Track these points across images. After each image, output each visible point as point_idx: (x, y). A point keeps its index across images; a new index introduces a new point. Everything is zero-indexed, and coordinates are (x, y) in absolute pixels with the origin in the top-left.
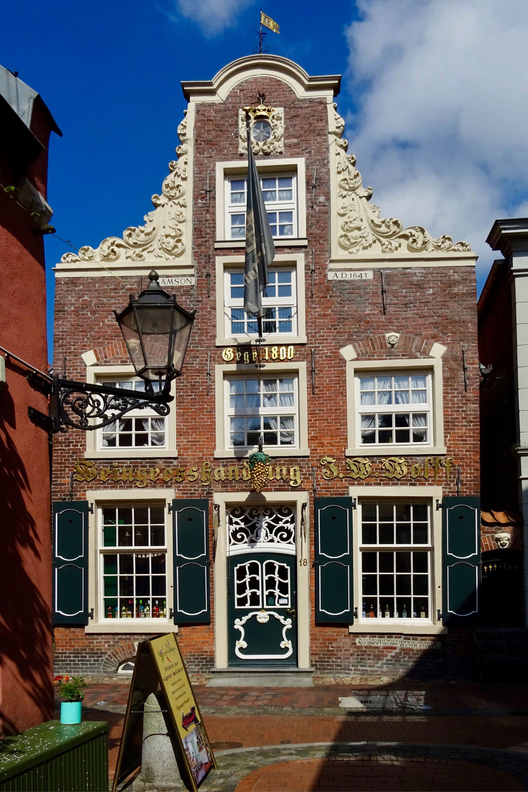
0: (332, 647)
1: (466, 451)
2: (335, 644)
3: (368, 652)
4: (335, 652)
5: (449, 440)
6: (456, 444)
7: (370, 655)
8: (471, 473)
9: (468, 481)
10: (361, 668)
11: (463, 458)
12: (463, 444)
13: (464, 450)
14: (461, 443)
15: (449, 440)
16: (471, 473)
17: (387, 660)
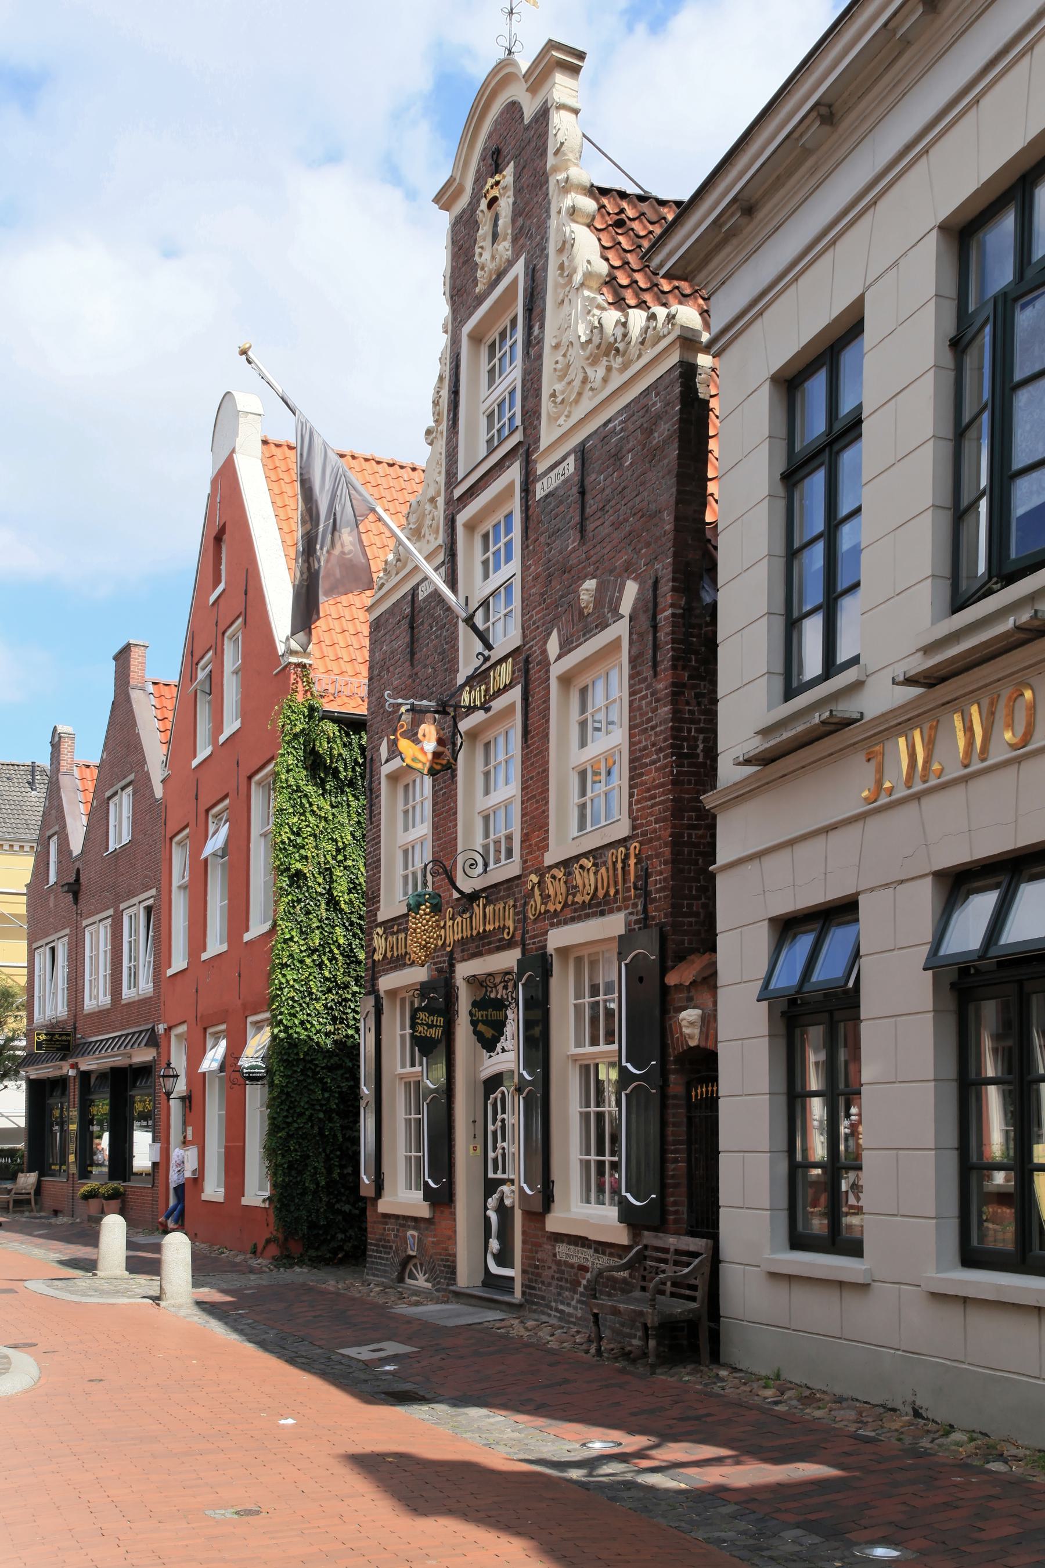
0: (538, 1260)
1: (656, 823)
2: (539, 1256)
3: (566, 1276)
4: (540, 1271)
5: (638, 802)
6: (643, 808)
7: (566, 1280)
8: (661, 873)
9: (658, 891)
10: (561, 1307)
11: (651, 840)
12: (652, 806)
13: (652, 819)
14: (649, 803)
15: (638, 802)
16: (661, 873)
17: (582, 1294)
